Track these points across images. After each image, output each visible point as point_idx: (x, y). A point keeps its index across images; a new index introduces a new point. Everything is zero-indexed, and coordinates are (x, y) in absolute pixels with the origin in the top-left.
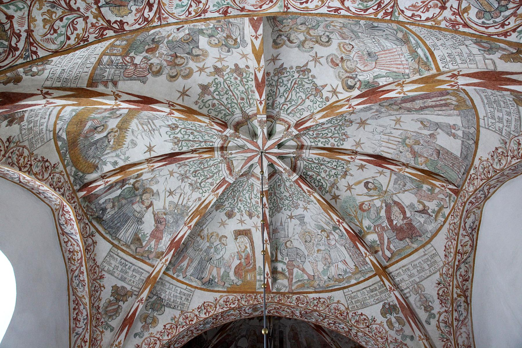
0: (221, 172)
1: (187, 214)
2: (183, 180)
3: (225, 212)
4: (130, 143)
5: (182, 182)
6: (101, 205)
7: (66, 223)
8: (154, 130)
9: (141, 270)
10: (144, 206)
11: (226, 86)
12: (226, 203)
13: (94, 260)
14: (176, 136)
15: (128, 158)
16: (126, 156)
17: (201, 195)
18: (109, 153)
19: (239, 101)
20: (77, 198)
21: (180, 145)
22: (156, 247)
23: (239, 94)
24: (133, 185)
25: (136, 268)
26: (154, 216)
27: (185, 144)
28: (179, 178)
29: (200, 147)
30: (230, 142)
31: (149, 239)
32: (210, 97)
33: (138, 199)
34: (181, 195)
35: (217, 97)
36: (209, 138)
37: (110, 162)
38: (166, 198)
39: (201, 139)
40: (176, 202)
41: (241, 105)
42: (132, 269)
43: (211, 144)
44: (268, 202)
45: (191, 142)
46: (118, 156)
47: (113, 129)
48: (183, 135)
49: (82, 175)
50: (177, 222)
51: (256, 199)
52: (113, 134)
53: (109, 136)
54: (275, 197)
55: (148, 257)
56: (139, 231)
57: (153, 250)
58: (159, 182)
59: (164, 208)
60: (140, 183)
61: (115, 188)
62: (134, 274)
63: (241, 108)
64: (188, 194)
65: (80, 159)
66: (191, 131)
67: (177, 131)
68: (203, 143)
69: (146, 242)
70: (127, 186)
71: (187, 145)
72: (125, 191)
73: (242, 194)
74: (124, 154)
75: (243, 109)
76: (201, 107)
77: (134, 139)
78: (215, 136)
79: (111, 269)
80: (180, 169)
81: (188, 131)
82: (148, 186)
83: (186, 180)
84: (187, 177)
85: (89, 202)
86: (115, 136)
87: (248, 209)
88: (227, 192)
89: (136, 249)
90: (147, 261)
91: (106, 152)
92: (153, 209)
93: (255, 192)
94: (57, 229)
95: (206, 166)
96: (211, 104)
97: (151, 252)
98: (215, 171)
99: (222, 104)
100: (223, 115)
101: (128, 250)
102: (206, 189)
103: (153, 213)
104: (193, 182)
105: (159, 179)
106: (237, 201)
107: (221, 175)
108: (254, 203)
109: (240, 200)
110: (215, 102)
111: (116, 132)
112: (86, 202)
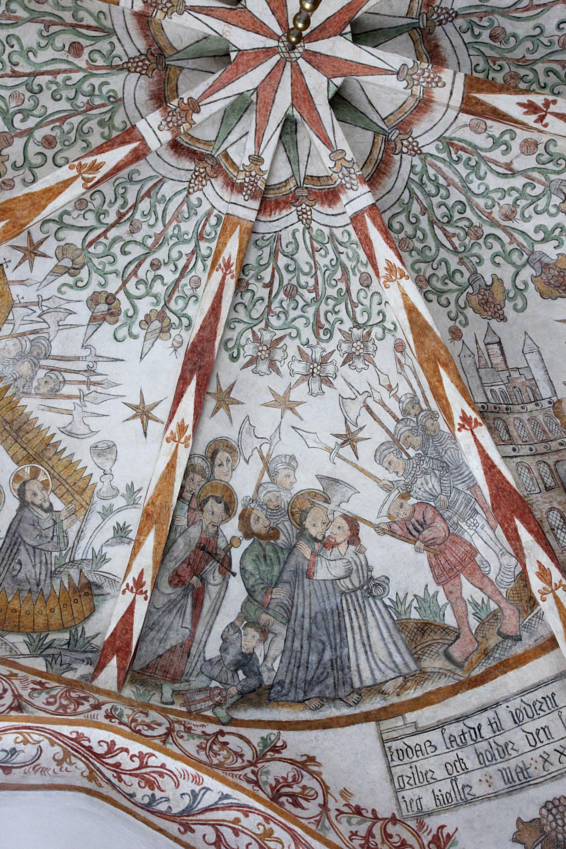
0: (338, 233)
1: (433, 416)
2: (326, 380)
3: (532, 294)
4: (98, 461)
5: (330, 385)
6: (220, 660)
7: (151, 785)
8: (90, 371)
9: (539, 694)
10: (343, 548)
11: (10, 82)
13: (358, 811)
14: (141, 317)
15: (130, 488)
16: (123, 490)
17: (388, 336)
18: (80, 531)
19: (81, 63)
20: (108, 693)
21: (174, 319)
22: (489, 589)
23: (48, 54)
24: (247, 536)
25: (516, 703)
26: (393, 533)
27: (181, 303)
28: (315, 386)
29: (209, 262)
30: (226, 156)
31: (448, 594)
32: (19, 143)
33: (305, 550)
34: (368, 408)
35: (31, 122)
36: (194, 220)
37: (107, 543)
38: (360, 463)
39: (187, 249)
40: (384, 437)
41: (100, 62)
42: (507, 722)
43: (213, 220)
44: (527, 91)
45: (184, 281)
46: (107, 513)
47: (17, 477)
48: (147, 294)
49: (67, 636)
50: (445, 467)
51: (515, 146)
52: (34, 486)
53: (29, 497)
54: (540, 67)
55: (506, 637)
56: (401, 609)
57: (493, 606)
58: (293, 458)
59: (388, 488)
60: (258, 512)
61: (213, 591)
62: (531, 727)
63: (111, 67)
64: (375, 384)
65: (15, 605)
66: (146, 265)
67: (125, 304)
68: (203, 245)
69: (449, 611)
70: (236, 554)
71: (187, 299)
72: (250, 567)
73: (481, 202)
74: (116, 492)
75: (117, 62)
76: (30, 178)
77: (93, 440)
78: (193, 198)
79: (446, 787)
80: (284, 369)
81: (141, 273)
82: (286, 498)
83: (330, 369)
84: (324, 361)
85: (174, 680)
86: (45, 485)
88: (431, 242)
89: (449, 657)
90: (518, 649)
91: (72, 535)
92: (370, 524)
93: (481, 141)
94: (160, 830)
95: (312, 282)
96: (41, 149)
97: (495, 615)
98: (332, 255)
99: (63, 120)
100: (98, 130)
101: (429, 687)
102: (375, 309)
103: (380, 530)
104: (345, 347)
105: (281, 449)
106: (504, 229)
107: (345, 239)
108: (530, 162)
109: (507, 218)
110: (39, 134)
111: (35, 474)
112: (160, 688)
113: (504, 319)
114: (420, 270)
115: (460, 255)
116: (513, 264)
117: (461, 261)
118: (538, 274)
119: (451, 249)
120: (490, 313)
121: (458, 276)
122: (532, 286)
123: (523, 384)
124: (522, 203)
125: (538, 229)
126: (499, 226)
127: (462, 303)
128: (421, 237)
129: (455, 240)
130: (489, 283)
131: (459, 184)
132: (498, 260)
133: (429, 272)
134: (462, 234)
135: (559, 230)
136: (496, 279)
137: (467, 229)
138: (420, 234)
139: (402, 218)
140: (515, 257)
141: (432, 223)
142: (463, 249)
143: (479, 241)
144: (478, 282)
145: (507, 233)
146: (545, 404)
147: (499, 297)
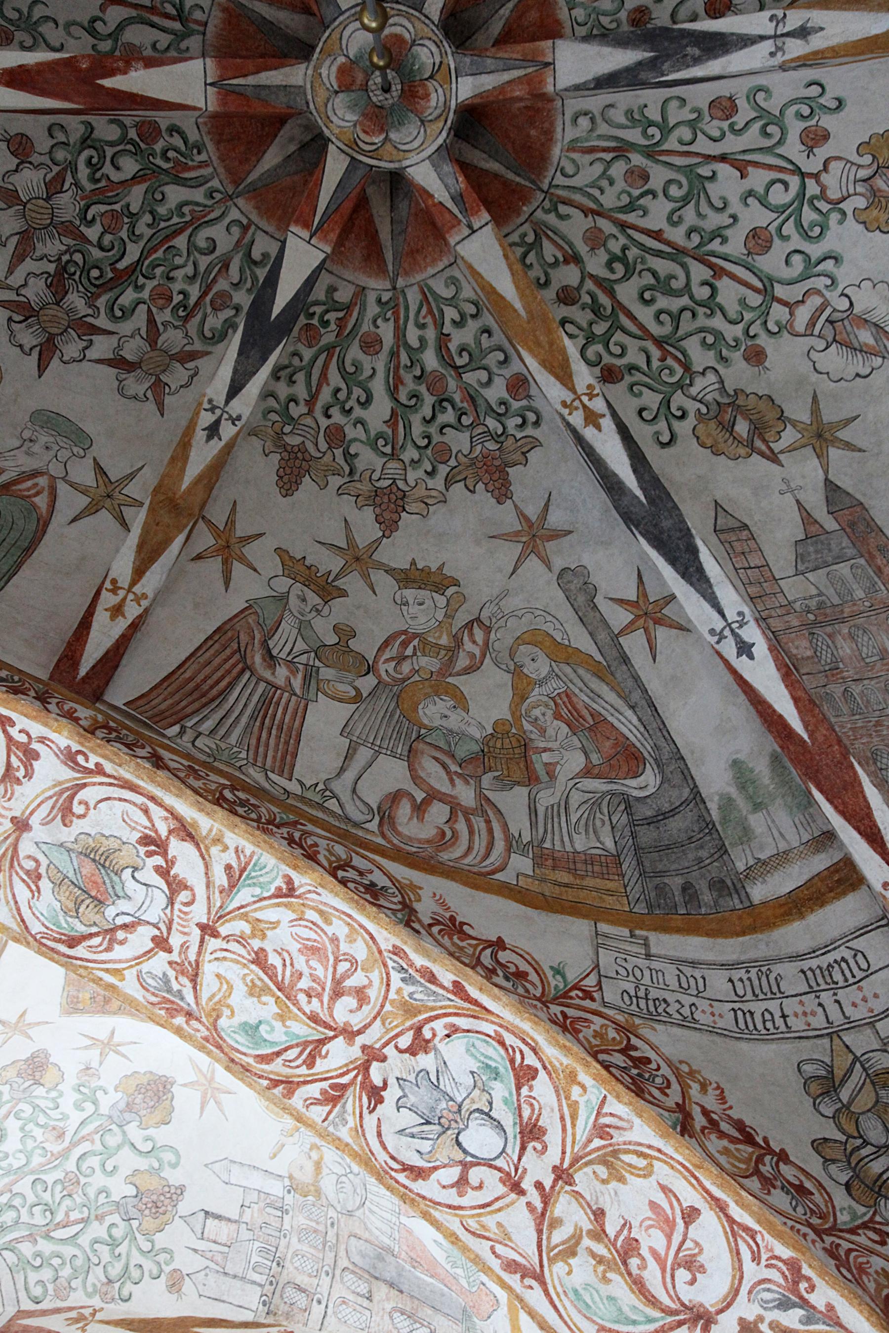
3: (162, 1134)
12: (121, 1189)
73: (36, 1160)
87: (40, 1091)
88: (68, 1251)
106: (74, 1144)
109: (61, 1136)
113: (182, 1189)
114: (94, 1285)
115: (92, 1217)
116: (119, 1147)
117: (100, 1218)
118: (138, 1118)
119: (81, 1226)
120: (170, 1208)
121: (117, 1233)
122: (151, 1132)
123: (261, 1211)
124: (42, 1120)
125: (78, 1107)
126: (68, 1150)
127: (146, 1246)
128: (59, 1261)
129: (74, 1216)
130: (134, 1193)
131: (12, 1178)
132: (109, 1168)
133: (99, 1270)
134: (67, 1202)
135: (82, 1088)
136: (133, 1178)
137: (65, 1193)
138: (56, 1262)
139: (33, 1277)
140: (112, 1141)
141: (47, 1236)
142: (85, 1209)
143: (82, 1183)
144: (129, 1207)
145: (79, 1142)
146: (289, 1199)
147: (154, 1184)
